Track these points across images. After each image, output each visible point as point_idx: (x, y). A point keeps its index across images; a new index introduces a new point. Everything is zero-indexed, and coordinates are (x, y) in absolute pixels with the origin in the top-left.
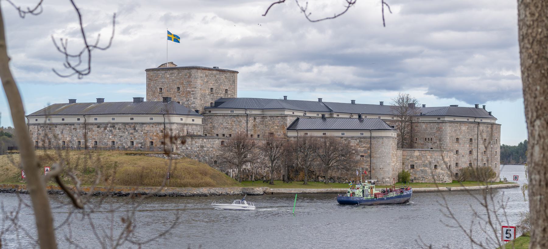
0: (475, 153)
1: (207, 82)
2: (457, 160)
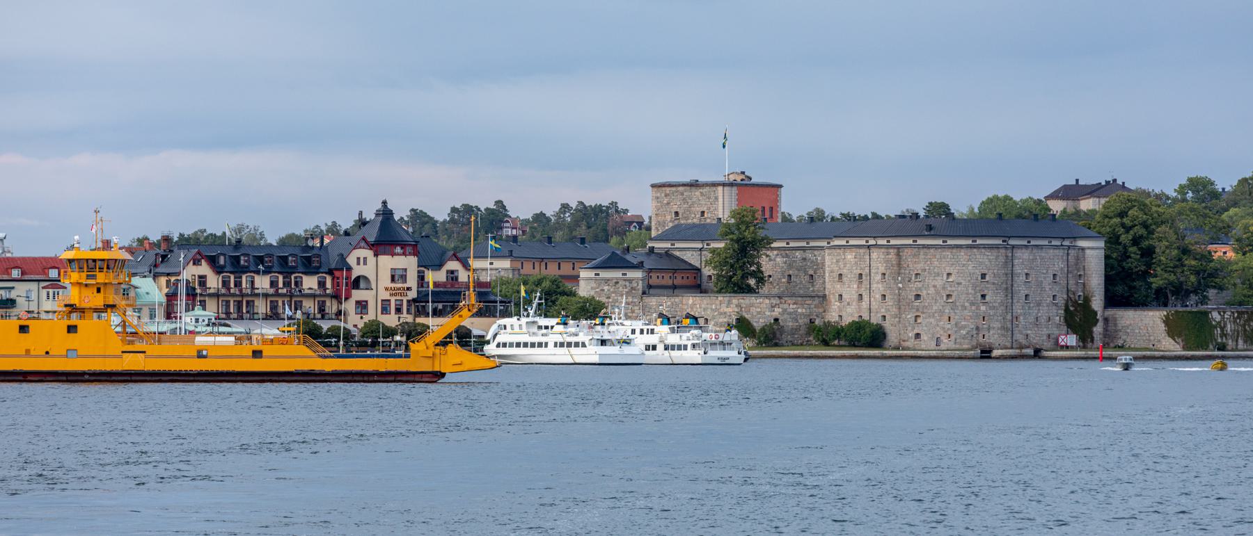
0: (866, 298)
2: (840, 310)
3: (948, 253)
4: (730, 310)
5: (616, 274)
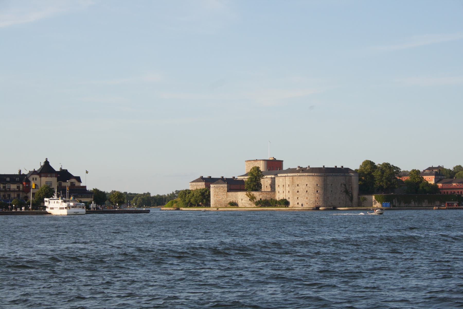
0: (285, 192)
3: (306, 178)
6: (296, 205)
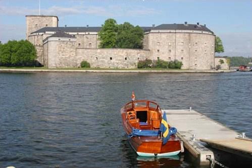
0: (173, 51)
1: (33, 22)
3: (205, 36)
4: (123, 54)
5: (67, 39)
6: (193, 68)
